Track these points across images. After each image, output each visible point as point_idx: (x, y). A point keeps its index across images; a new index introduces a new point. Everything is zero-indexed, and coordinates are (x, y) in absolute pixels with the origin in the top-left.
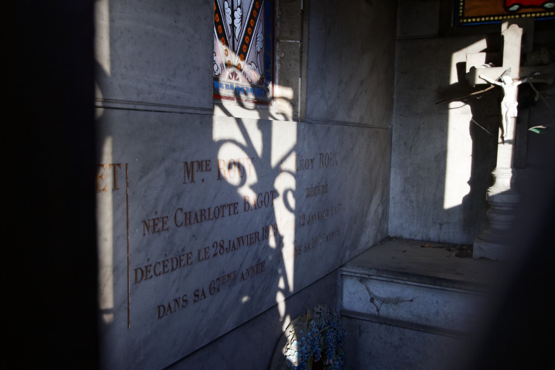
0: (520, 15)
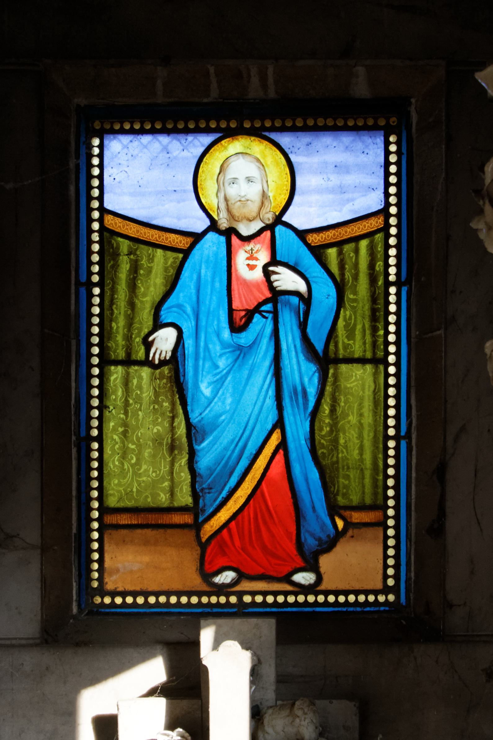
0: (240, 595)
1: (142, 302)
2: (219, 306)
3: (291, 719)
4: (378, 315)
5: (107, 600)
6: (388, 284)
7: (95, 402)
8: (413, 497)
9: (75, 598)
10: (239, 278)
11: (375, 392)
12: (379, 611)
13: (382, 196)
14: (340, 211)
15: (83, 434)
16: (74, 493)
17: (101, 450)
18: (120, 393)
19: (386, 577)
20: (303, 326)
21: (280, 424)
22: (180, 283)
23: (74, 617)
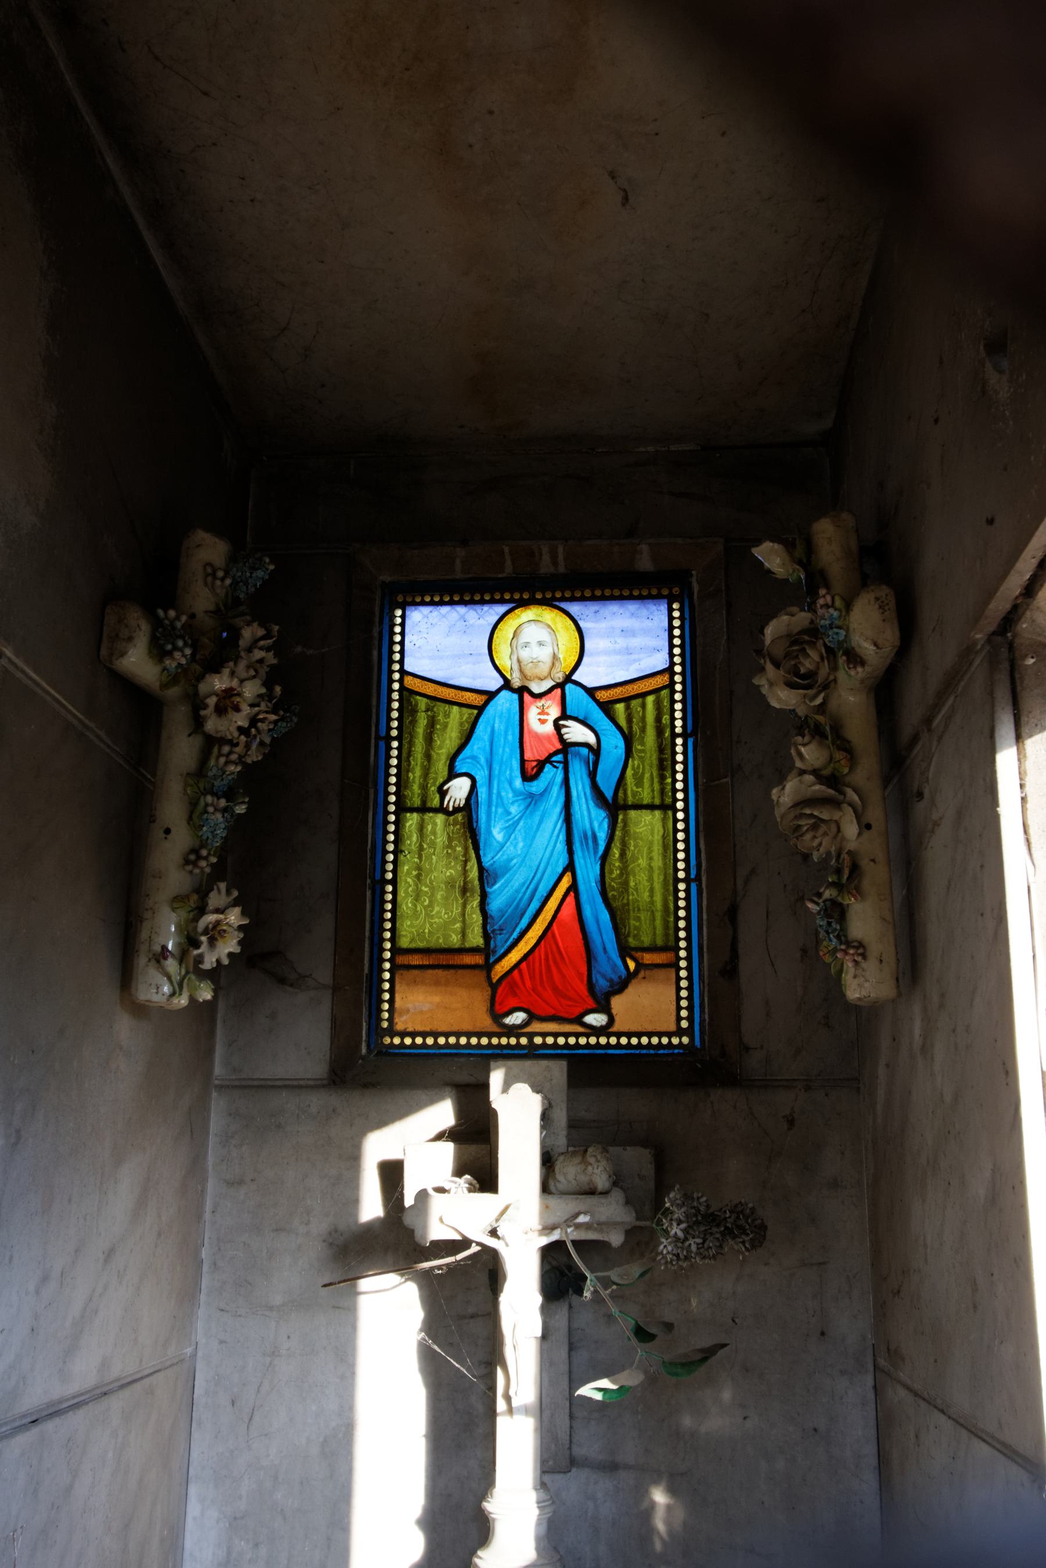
0: (531, 1036)
1: (438, 754)
2: (511, 757)
3: (583, 1167)
4: (665, 764)
5: (397, 1041)
6: (674, 736)
7: (391, 847)
8: (705, 938)
9: (364, 1038)
10: (530, 731)
11: (664, 837)
12: (673, 1054)
13: (667, 656)
14: (627, 670)
15: (378, 877)
16: (367, 934)
17: (394, 893)
18: (414, 839)
19: (679, 1019)
20: (592, 775)
21: (570, 867)
22: (475, 736)
23: (363, 1058)
